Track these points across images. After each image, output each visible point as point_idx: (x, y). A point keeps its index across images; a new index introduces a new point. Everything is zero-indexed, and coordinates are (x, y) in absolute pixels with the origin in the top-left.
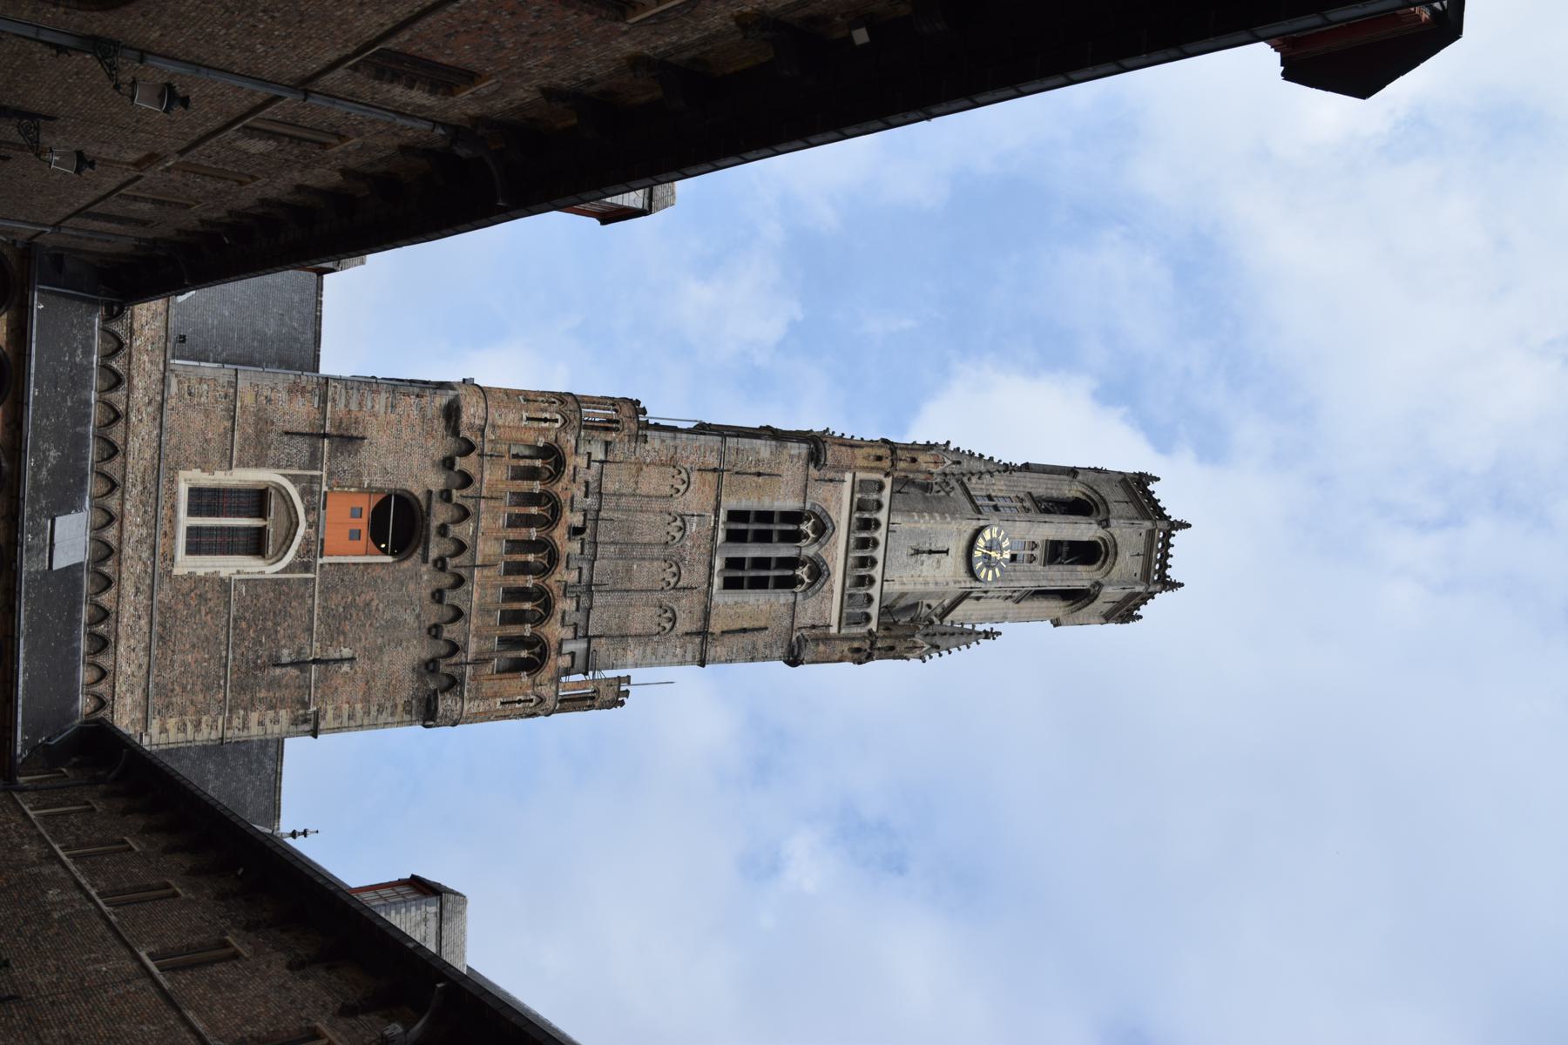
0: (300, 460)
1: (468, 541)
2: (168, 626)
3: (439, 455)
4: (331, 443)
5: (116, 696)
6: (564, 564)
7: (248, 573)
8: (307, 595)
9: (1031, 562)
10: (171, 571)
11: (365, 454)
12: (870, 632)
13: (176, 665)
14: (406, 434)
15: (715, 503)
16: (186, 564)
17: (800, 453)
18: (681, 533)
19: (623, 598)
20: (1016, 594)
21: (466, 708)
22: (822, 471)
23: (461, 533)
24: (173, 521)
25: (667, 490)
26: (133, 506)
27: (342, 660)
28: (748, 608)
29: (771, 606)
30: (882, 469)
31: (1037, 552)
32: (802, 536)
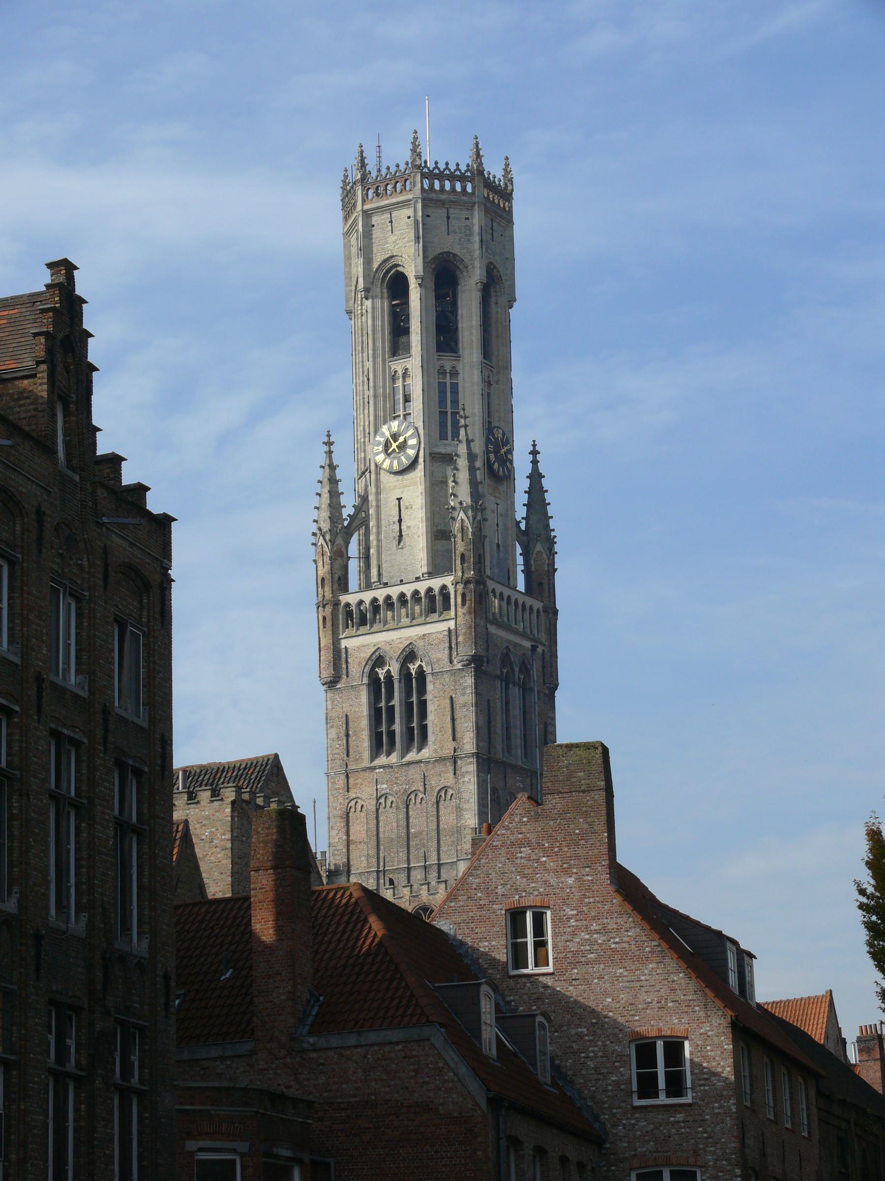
15: (368, 771)
18: (389, 797)
25: (363, 814)
29: (435, 697)
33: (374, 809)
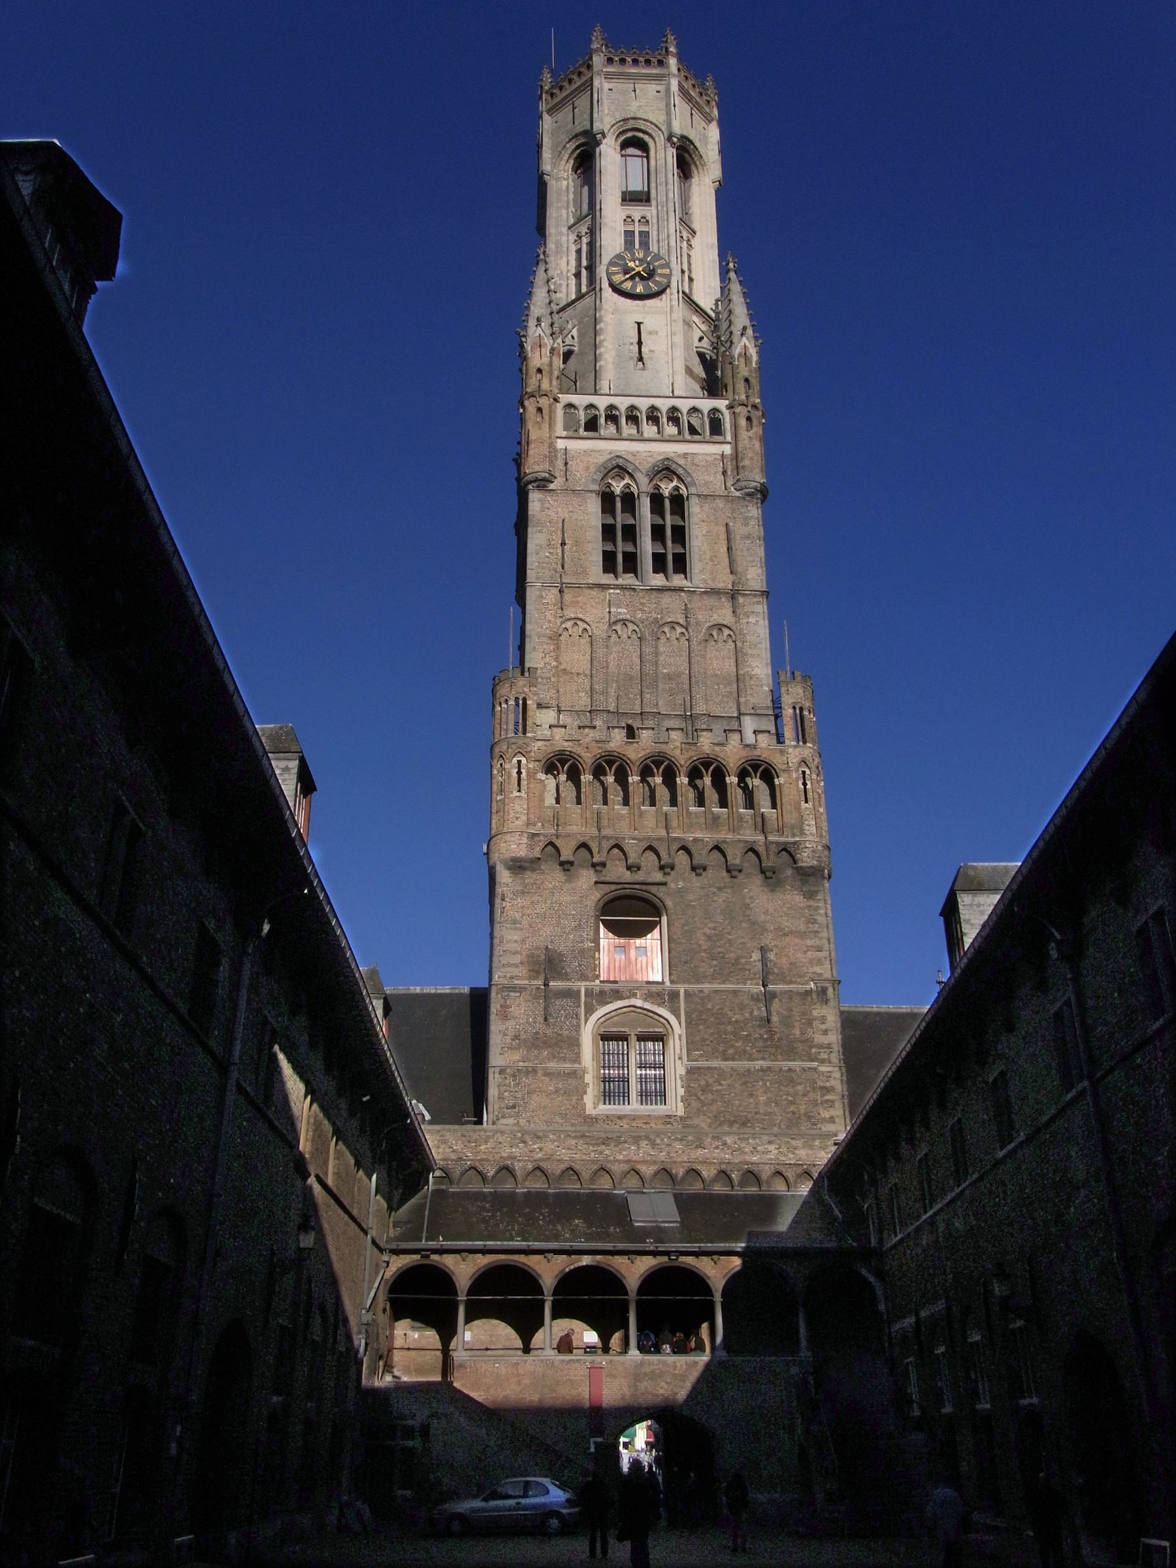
0: (570, 1006)
1: (645, 845)
2: (732, 1118)
3: (558, 875)
4: (554, 979)
5: (799, 1162)
6: (663, 746)
7: (681, 1049)
8: (701, 995)
9: (648, 221)
10: (680, 1117)
11: (562, 947)
12: (730, 407)
13: (769, 1110)
14: (541, 908)
15: (596, 589)
16: (675, 1105)
17: (539, 500)
19: (697, 682)
20: (685, 234)
21: (811, 838)
22: (557, 474)
23: (636, 852)
24: (634, 1118)
25: (585, 640)
26: (620, 1153)
27: (764, 960)
28: (705, 548)
29: (703, 521)
30: (550, 406)
31: (637, 217)
32: (627, 490)
33: (604, 635)
